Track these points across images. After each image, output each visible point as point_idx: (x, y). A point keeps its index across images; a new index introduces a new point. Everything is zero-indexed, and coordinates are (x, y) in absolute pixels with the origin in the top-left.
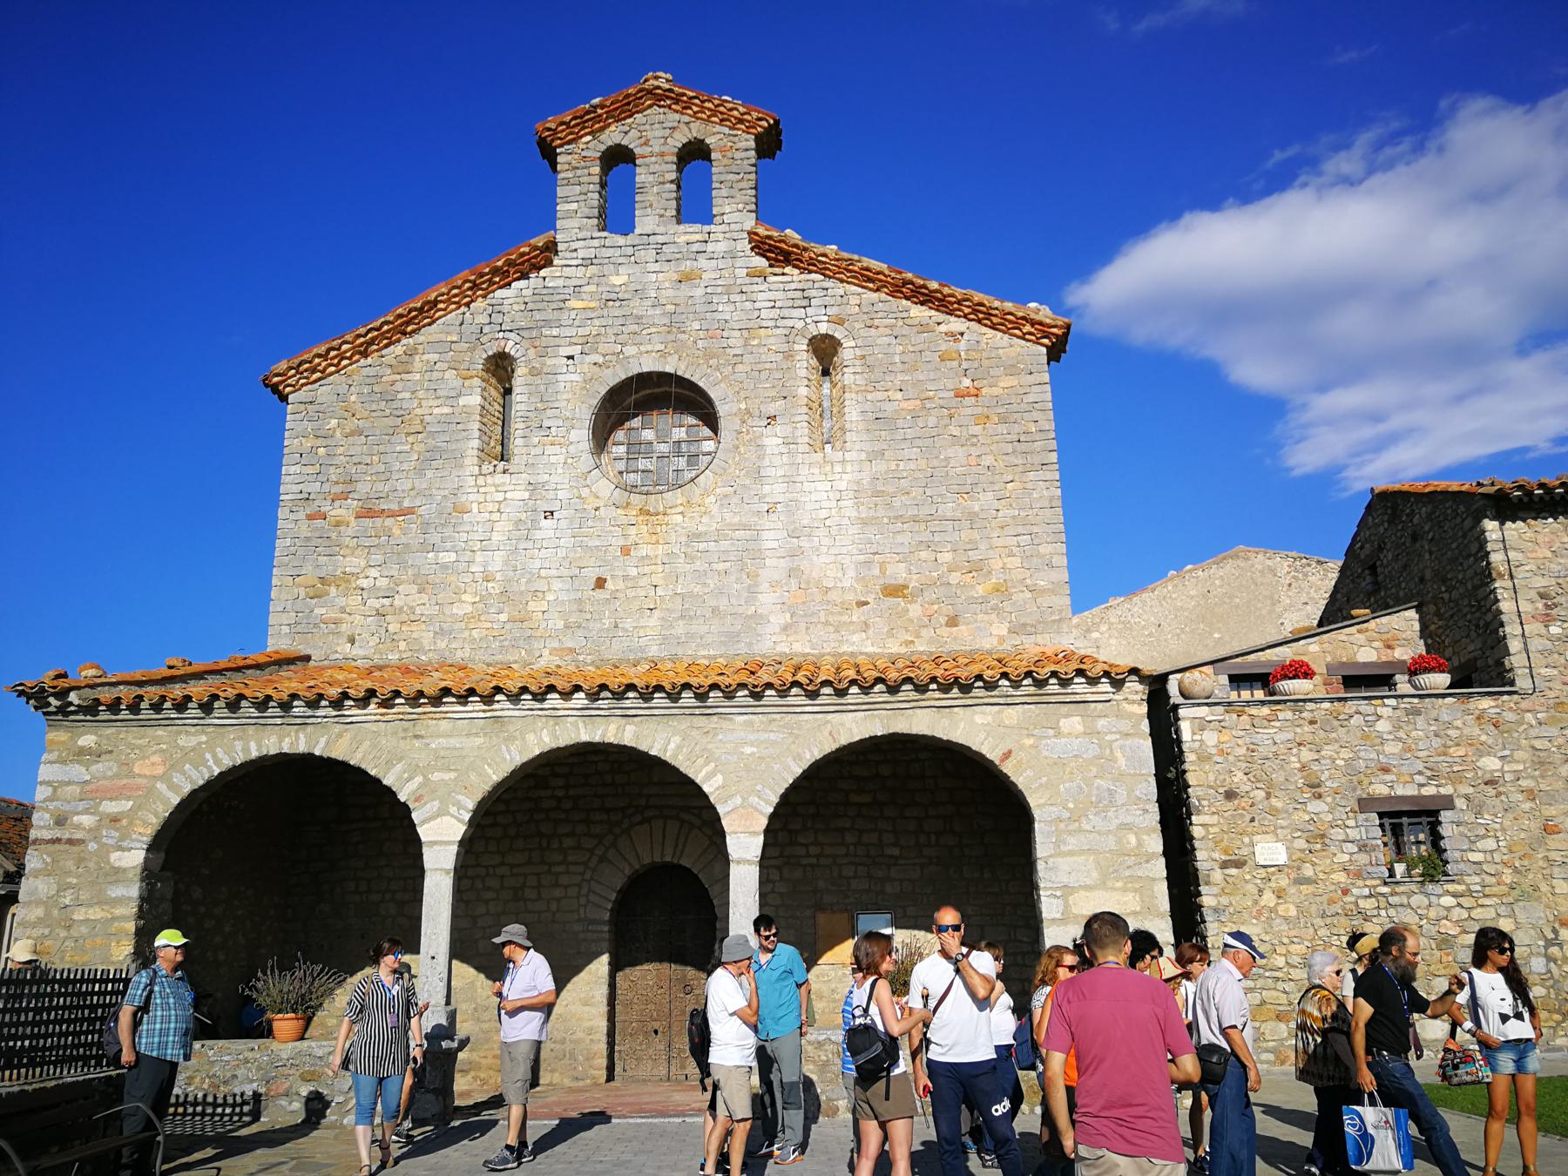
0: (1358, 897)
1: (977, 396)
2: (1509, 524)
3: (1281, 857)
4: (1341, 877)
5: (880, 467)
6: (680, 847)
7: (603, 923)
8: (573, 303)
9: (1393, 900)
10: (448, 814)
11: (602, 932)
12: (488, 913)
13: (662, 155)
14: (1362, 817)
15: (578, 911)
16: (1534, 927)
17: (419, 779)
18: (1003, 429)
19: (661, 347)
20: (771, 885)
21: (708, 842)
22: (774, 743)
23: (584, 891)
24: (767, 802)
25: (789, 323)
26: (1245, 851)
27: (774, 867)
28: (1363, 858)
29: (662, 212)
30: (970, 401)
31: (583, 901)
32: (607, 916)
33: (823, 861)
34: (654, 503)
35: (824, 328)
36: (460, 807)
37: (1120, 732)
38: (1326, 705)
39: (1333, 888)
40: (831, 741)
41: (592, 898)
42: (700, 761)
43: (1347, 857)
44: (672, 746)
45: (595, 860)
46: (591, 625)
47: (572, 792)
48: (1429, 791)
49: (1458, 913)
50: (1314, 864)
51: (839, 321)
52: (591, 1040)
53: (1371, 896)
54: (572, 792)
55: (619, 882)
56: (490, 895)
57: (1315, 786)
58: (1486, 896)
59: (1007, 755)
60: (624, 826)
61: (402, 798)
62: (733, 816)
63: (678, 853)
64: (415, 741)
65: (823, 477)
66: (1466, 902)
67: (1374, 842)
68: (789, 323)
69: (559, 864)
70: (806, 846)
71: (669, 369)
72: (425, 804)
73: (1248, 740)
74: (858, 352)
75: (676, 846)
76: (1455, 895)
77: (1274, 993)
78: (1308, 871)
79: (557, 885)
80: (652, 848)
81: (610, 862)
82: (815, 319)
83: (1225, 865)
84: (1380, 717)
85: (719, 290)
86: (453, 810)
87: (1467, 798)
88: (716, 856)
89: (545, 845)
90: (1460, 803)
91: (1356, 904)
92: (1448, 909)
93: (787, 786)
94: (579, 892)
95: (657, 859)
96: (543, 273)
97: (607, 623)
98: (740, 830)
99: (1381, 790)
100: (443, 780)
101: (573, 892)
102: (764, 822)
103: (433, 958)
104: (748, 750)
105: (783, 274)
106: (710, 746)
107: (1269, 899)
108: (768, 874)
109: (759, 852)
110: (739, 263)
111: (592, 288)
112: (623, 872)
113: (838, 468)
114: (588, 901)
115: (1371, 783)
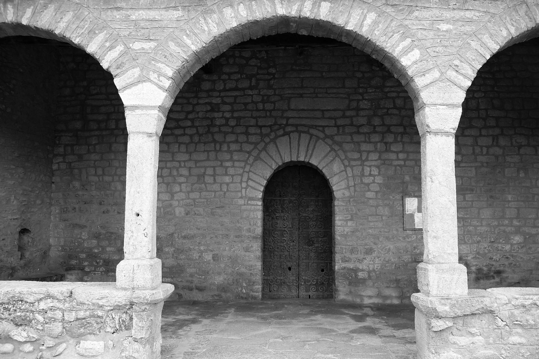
6: (310, 152)
7: (258, 200)
10: (149, 80)
11: (257, 205)
12: (181, 191)
15: (241, 191)
17: (120, 48)
20: (373, 178)
21: (329, 149)
22: (470, 21)
23: (245, 179)
24: (465, 76)
27: (374, 166)
31: (244, 185)
32: (260, 195)
33: (408, 163)
36: (160, 74)
40: (528, 20)
41: (251, 183)
42: (397, 36)
45: (251, 159)
47: (236, 115)
52: (251, 274)
54: (236, 115)
55: (268, 174)
56: (182, 179)
60: (271, 137)
61: (105, 65)
62: (431, 89)
63: (308, 156)
64: (115, 13)
69: (227, 161)
70: (397, 153)
72: (127, 71)
75: (307, 150)
79: (226, 174)
80: (291, 151)
81: (261, 159)
86: (153, 76)
88: (334, 158)
89: (218, 148)
93: (484, 61)
94: (241, 180)
95: (294, 159)
98: (440, 102)
100: (143, 49)
101: (238, 179)
102: (461, 96)
103: (138, 215)
104: (444, 27)
106: (407, 22)
108: (371, 171)
109: (456, 125)
112: (271, 167)
114: (248, 185)
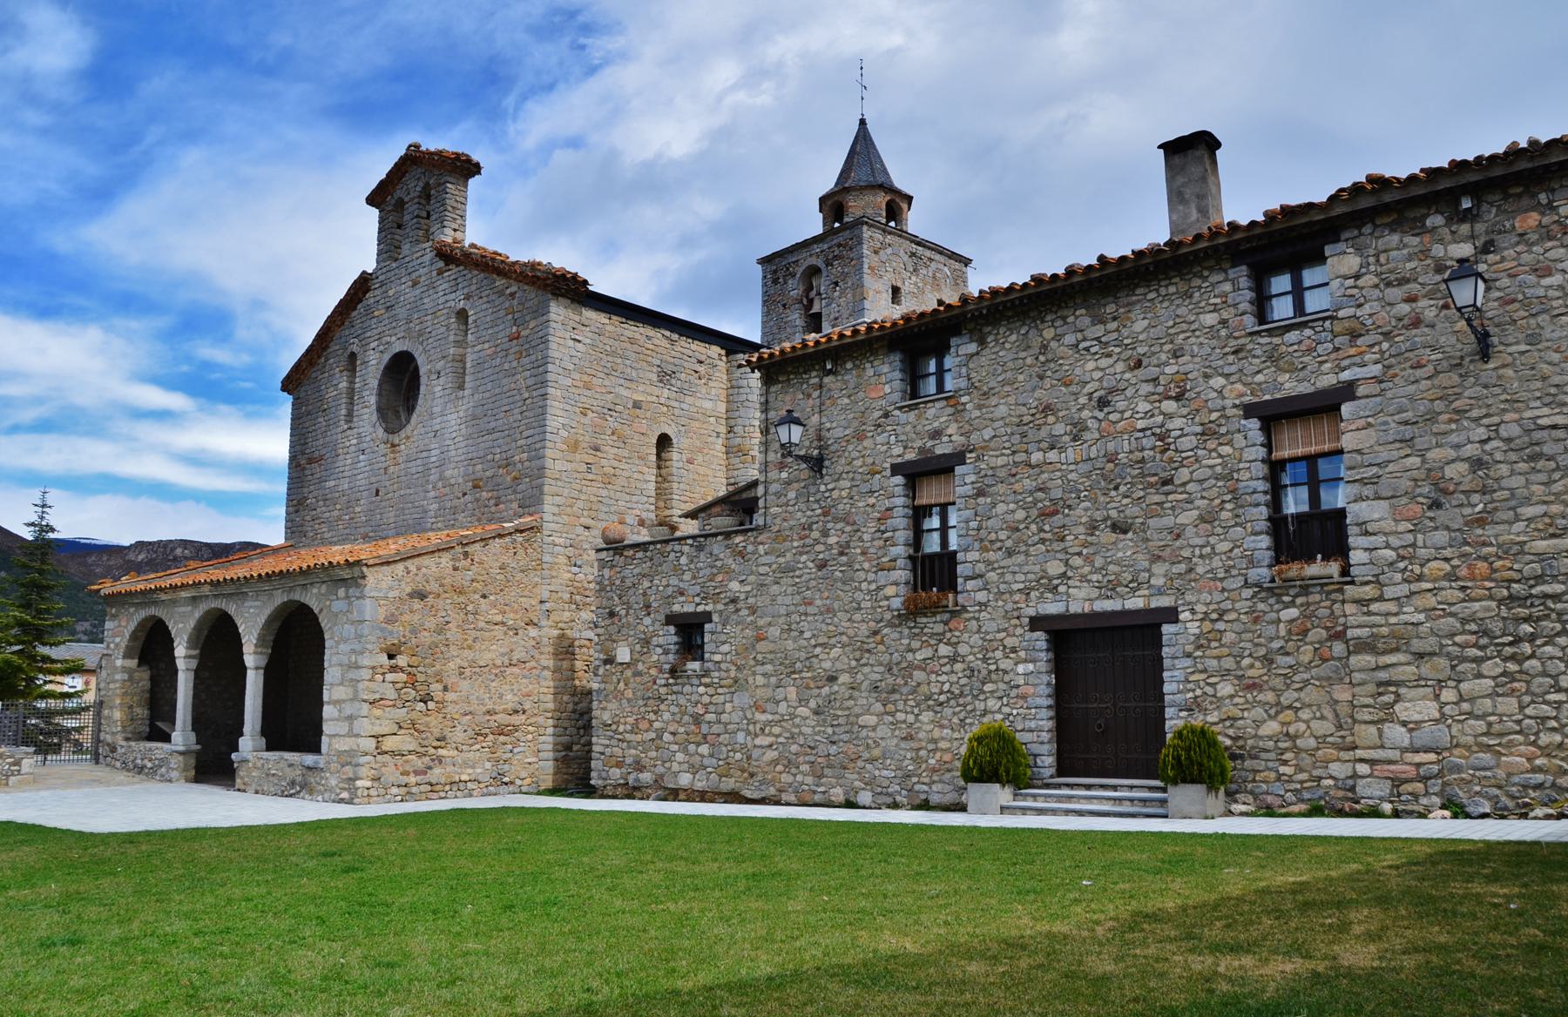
1: (517, 338)
2: (773, 389)
3: (627, 659)
4: (653, 672)
8: (376, 313)
9: (675, 688)
13: (413, 199)
16: (743, 710)
18: (526, 360)
25: (448, 305)
38: (659, 546)
48: (700, 609)
49: (706, 699)
51: (467, 297)
59: (321, 611)
66: (711, 691)
68: (448, 305)
78: (640, 667)
83: (606, 662)
87: (721, 612)
90: (715, 618)
99: (676, 608)
107: (622, 685)
110: (434, 267)
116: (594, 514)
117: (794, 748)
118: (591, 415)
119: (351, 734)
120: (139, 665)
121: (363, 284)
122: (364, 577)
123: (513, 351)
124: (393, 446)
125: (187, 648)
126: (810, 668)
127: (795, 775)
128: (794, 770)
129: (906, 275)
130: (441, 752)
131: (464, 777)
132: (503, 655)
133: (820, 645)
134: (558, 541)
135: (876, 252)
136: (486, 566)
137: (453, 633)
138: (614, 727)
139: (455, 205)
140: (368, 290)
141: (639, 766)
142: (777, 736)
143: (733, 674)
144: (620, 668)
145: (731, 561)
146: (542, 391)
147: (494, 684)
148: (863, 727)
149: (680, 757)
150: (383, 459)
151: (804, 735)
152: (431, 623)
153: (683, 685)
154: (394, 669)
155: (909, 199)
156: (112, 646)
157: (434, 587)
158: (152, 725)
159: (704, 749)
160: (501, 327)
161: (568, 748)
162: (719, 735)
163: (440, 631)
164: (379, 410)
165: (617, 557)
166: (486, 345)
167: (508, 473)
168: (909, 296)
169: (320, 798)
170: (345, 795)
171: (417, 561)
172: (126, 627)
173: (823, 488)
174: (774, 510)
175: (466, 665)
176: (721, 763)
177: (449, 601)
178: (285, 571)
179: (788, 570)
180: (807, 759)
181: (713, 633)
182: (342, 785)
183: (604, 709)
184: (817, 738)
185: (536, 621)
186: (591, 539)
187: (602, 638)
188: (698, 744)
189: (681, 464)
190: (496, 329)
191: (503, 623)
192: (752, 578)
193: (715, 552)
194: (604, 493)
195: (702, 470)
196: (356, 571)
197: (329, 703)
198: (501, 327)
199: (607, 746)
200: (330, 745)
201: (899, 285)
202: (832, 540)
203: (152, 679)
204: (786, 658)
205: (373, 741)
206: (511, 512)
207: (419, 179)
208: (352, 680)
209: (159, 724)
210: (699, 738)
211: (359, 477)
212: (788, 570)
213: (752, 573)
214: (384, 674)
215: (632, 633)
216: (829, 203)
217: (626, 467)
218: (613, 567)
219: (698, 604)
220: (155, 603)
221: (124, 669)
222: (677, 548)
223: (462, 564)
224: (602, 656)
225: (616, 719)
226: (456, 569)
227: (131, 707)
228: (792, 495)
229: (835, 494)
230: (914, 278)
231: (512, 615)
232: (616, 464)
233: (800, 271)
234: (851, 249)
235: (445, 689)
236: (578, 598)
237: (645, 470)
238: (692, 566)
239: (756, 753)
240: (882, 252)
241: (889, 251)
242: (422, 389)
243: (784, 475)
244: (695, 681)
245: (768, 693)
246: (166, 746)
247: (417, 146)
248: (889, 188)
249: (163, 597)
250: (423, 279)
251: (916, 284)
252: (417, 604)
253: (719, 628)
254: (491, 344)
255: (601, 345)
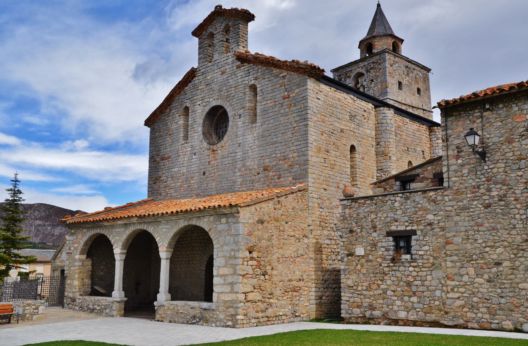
0: (384, 267)
1: (288, 98)
2: (449, 119)
3: (363, 253)
4: (379, 260)
5: (264, 126)
7: (204, 271)
8: (200, 88)
9: (394, 268)
13: (219, 32)
14: (387, 238)
16: (438, 279)
18: (295, 108)
19: (217, 97)
22: (168, 228)
25: (244, 82)
26: (353, 251)
28: (386, 253)
29: (219, 52)
30: (287, 100)
32: (204, 269)
34: (215, 148)
35: (253, 82)
37: (233, 222)
38: (380, 198)
39: (377, 263)
43: (381, 253)
44: (152, 229)
46: (202, 186)
48: (409, 228)
49: (415, 274)
50: (373, 255)
51: (256, 79)
53: (387, 267)
54: (198, 234)
57: (374, 227)
58: (423, 267)
59: (210, 230)
65: (250, 133)
66: (417, 269)
67: (390, 247)
68: (244, 82)
71: (219, 104)
73: (357, 212)
74: (260, 88)
76: (414, 267)
77: (357, 299)
78: (371, 257)
82: (251, 79)
83: (348, 255)
84: (396, 201)
85: (230, 75)
87: (422, 230)
90: (419, 233)
91: (383, 269)
92: (411, 272)
96: (194, 79)
97: (205, 185)
99: (393, 228)
104: (164, 230)
105: (244, 66)
107: (359, 267)
110: (234, 65)
111: (204, 82)
113: (254, 130)
115: (391, 226)
116: (328, 183)
117: (475, 299)
118: (325, 135)
119: (232, 292)
120: (87, 258)
121: (191, 75)
122: (238, 213)
123: (286, 104)
124: (213, 151)
125: (121, 249)
126: (482, 259)
127: (476, 314)
128: (475, 311)
129: (404, 76)
130: (271, 301)
131: (281, 313)
132: (295, 252)
133: (489, 246)
134: (315, 196)
135: (391, 66)
136: (287, 208)
137: (275, 241)
138: (355, 288)
139: (243, 35)
140: (195, 77)
141: (372, 308)
142: (462, 293)
143: (431, 261)
144: (358, 258)
145: (427, 204)
146: (305, 123)
147: (291, 266)
148: (522, 289)
149: (398, 303)
150: (207, 157)
151: (481, 292)
152: (266, 236)
153: (399, 267)
154: (252, 259)
155: (402, 41)
156: (72, 248)
157: (266, 218)
158: (92, 288)
159: (414, 299)
160: (278, 93)
161: (321, 298)
162: (423, 292)
163: (270, 240)
164: (204, 134)
165: (354, 203)
166: (269, 102)
167: (285, 163)
168: (405, 86)
169: (214, 325)
170: (230, 323)
171: (260, 205)
172: (81, 239)
173: (486, 167)
174: (454, 179)
175: (280, 257)
176: (425, 306)
177: (273, 225)
178: (189, 210)
179: (464, 208)
180: (484, 305)
181: (417, 240)
182: (228, 318)
183: (348, 278)
184: (490, 294)
185: (307, 235)
186: (327, 195)
187: (346, 243)
188: (410, 297)
189: (359, 160)
190: (275, 94)
191: (294, 236)
192: (441, 213)
193: (417, 200)
194: (331, 173)
195: (367, 163)
196: (234, 210)
197: (217, 276)
198: (278, 93)
199: (351, 297)
200: (218, 298)
201: (401, 81)
202: (494, 193)
203: (93, 265)
204: (466, 253)
205: (244, 295)
206: (288, 182)
207: (222, 23)
208: (232, 264)
209: (95, 287)
210: (411, 293)
211: (193, 166)
212: (464, 208)
213: (441, 210)
214: (248, 261)
215: (364, 241)
216: (365, 43)
217: (339, 160)
218: (350, 208)
219: (407, 226)
220: (100, 227)
221: (80, 260)
222: (392, 198)
223: (278, 206)
224: (346, 252)
225: (356, 284)
226: (275, 209)
227: (83, 279)
228: (465, 171)
229: (495, 170)
230: (407, 78)
231: (297, 232)
232: (335, 159)
233: (353, 75)
234: (380, 64)
235: (272, 269)
236: (323, 224)
237: (346, 162)
238: (402, 207)
239: (448, 302)
240: (394, 66)
241: (397, 65)
242: (230, 123)
243: (460, 161)
244: (407, 265)
245: (456, 271)
246: (108, 299)
247: (220, 7)
248: (392, 36)
249: (106, 224)
250: (227, 71)
251: (408, 80)
252: (260, 226)
253: (421, 238)
254: (272, 101)
255: (328, 102)
